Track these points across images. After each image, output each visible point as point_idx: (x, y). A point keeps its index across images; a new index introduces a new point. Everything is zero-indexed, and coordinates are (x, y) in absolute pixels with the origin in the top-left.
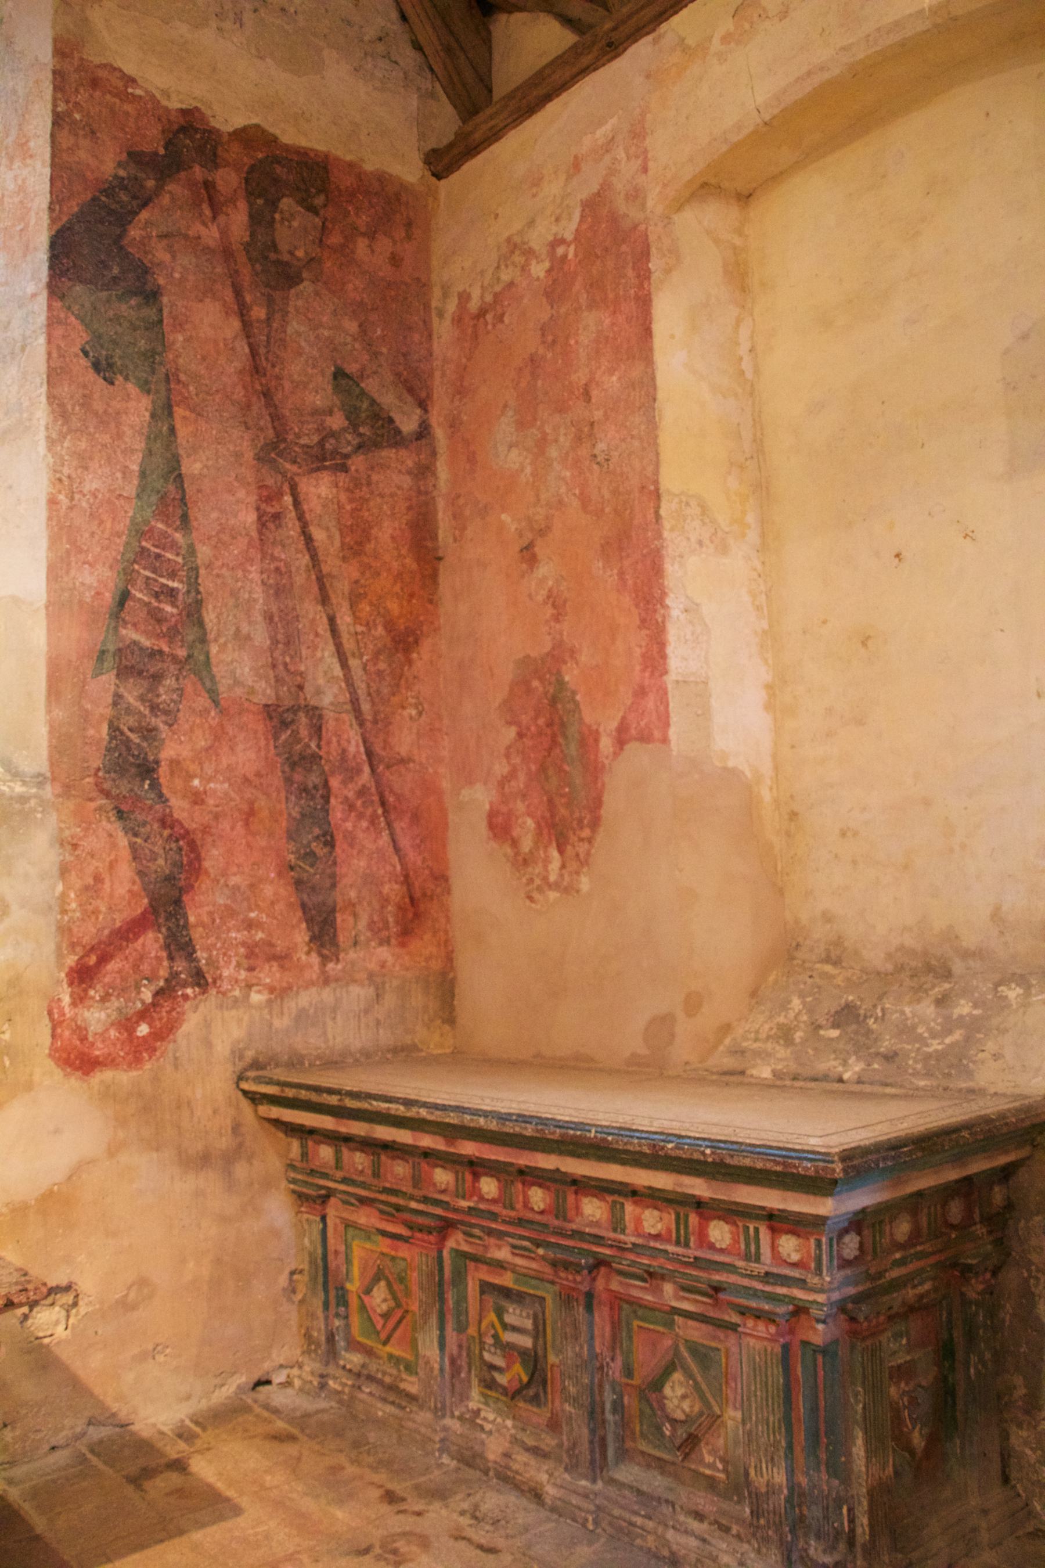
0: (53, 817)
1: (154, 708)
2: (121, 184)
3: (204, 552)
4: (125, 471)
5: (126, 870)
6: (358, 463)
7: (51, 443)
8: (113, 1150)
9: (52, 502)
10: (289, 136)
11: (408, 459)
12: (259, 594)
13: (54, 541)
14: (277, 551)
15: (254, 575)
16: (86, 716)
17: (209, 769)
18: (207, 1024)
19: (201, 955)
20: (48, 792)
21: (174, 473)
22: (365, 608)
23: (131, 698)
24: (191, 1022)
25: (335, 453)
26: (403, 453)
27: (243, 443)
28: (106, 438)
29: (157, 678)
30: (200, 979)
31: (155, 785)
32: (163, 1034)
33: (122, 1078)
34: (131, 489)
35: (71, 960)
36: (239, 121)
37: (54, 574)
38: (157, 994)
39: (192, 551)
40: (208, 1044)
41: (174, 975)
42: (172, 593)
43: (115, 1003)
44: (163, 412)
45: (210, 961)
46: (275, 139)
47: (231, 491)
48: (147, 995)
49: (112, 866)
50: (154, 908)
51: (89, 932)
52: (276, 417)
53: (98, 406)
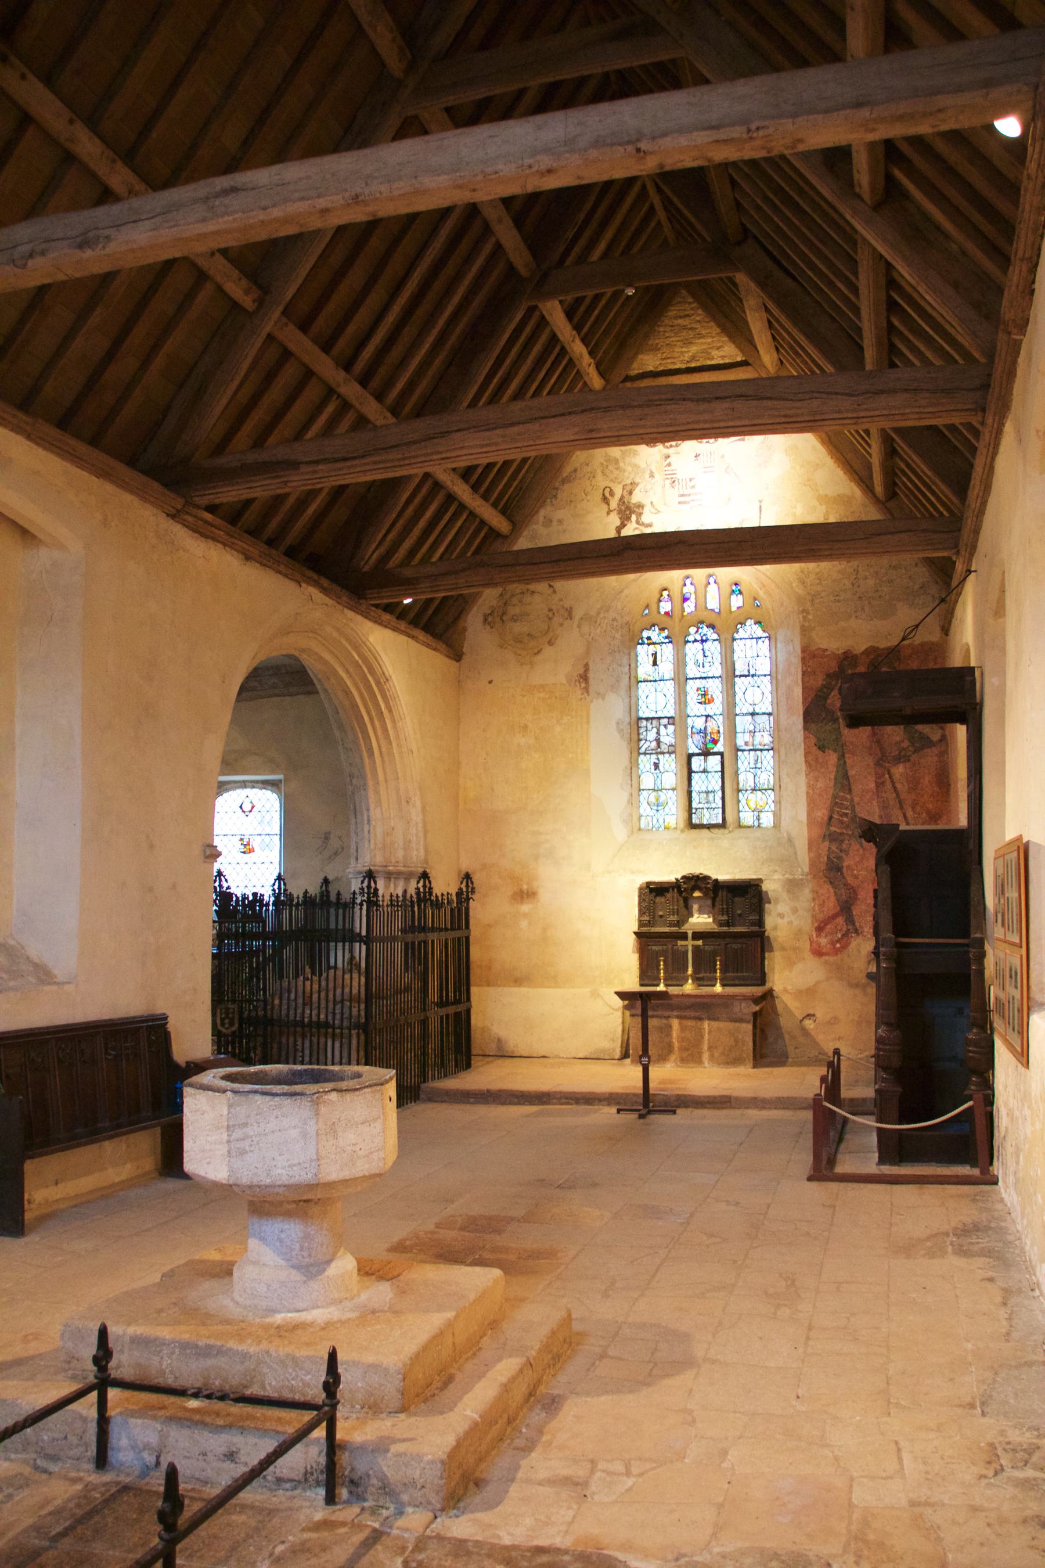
0: (811, 885)
1: (841, 851)
2: (824, 686)
3: (856, 799)
4: (830, 779)
5: (833, 898)
6: (914, 758)
7: (807, 775)
8: (827, 979)
9: (808, 793)
10: (883, 644)
11: (935, 750)
12: (877, 810)
13: (809, 804)
14: (884, 795)
15: (875, 803)
16: (820, 855)
17: (859, 867)
18: (859, 945)
19: (857, 924)
20: (809, 877)
21: (846, 776)
22: (918, 808)
23: (834, 848)
24: (854, 944)
25: (904, 756)
26: (934, 749)
27: (870, 761)
28: (823, 770)
29: (842, 841)
30: (856, 932)
31: (842, 874)
32: (844, 947)
33: (832, 959)
34: (832, 784)
35: (816, 925)
36: (864, 648)
37: (809, 815)
38: (843, 935)
39: (852, 800)
40: (859, 951)
41: (848, 930)
42: (846, 815)
43: (829, 937)
44: (842, 757)
45: (862, 927)
46: (878, 648)
47: (865, 777)
48: (839, 936)
49: (828, 898)
50: (842, 910)
51: (821, 917)
52: (882, 749)
53: (821, 760)
